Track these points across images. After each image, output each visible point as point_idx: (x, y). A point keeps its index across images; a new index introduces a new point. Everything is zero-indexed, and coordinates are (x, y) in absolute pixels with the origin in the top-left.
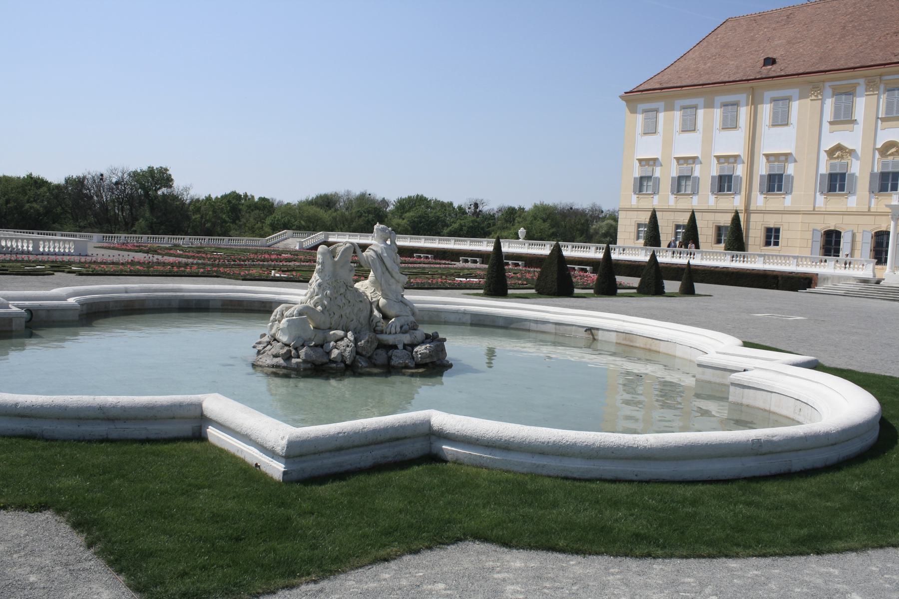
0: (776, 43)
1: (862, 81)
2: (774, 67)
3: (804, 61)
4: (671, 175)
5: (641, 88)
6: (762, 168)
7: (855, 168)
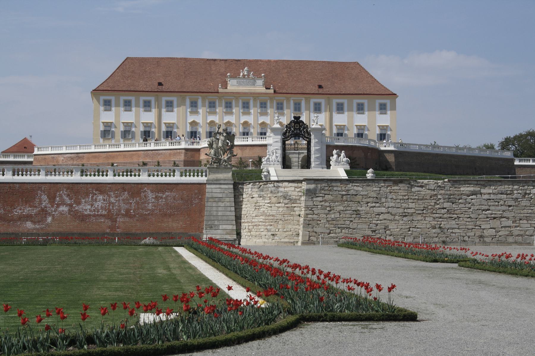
0: (158, 75)
1: (200, 97)
2: (163, 87)
3: (175, 86)
4: (120, 130)
5: (100, 88)
6: (164, 129)
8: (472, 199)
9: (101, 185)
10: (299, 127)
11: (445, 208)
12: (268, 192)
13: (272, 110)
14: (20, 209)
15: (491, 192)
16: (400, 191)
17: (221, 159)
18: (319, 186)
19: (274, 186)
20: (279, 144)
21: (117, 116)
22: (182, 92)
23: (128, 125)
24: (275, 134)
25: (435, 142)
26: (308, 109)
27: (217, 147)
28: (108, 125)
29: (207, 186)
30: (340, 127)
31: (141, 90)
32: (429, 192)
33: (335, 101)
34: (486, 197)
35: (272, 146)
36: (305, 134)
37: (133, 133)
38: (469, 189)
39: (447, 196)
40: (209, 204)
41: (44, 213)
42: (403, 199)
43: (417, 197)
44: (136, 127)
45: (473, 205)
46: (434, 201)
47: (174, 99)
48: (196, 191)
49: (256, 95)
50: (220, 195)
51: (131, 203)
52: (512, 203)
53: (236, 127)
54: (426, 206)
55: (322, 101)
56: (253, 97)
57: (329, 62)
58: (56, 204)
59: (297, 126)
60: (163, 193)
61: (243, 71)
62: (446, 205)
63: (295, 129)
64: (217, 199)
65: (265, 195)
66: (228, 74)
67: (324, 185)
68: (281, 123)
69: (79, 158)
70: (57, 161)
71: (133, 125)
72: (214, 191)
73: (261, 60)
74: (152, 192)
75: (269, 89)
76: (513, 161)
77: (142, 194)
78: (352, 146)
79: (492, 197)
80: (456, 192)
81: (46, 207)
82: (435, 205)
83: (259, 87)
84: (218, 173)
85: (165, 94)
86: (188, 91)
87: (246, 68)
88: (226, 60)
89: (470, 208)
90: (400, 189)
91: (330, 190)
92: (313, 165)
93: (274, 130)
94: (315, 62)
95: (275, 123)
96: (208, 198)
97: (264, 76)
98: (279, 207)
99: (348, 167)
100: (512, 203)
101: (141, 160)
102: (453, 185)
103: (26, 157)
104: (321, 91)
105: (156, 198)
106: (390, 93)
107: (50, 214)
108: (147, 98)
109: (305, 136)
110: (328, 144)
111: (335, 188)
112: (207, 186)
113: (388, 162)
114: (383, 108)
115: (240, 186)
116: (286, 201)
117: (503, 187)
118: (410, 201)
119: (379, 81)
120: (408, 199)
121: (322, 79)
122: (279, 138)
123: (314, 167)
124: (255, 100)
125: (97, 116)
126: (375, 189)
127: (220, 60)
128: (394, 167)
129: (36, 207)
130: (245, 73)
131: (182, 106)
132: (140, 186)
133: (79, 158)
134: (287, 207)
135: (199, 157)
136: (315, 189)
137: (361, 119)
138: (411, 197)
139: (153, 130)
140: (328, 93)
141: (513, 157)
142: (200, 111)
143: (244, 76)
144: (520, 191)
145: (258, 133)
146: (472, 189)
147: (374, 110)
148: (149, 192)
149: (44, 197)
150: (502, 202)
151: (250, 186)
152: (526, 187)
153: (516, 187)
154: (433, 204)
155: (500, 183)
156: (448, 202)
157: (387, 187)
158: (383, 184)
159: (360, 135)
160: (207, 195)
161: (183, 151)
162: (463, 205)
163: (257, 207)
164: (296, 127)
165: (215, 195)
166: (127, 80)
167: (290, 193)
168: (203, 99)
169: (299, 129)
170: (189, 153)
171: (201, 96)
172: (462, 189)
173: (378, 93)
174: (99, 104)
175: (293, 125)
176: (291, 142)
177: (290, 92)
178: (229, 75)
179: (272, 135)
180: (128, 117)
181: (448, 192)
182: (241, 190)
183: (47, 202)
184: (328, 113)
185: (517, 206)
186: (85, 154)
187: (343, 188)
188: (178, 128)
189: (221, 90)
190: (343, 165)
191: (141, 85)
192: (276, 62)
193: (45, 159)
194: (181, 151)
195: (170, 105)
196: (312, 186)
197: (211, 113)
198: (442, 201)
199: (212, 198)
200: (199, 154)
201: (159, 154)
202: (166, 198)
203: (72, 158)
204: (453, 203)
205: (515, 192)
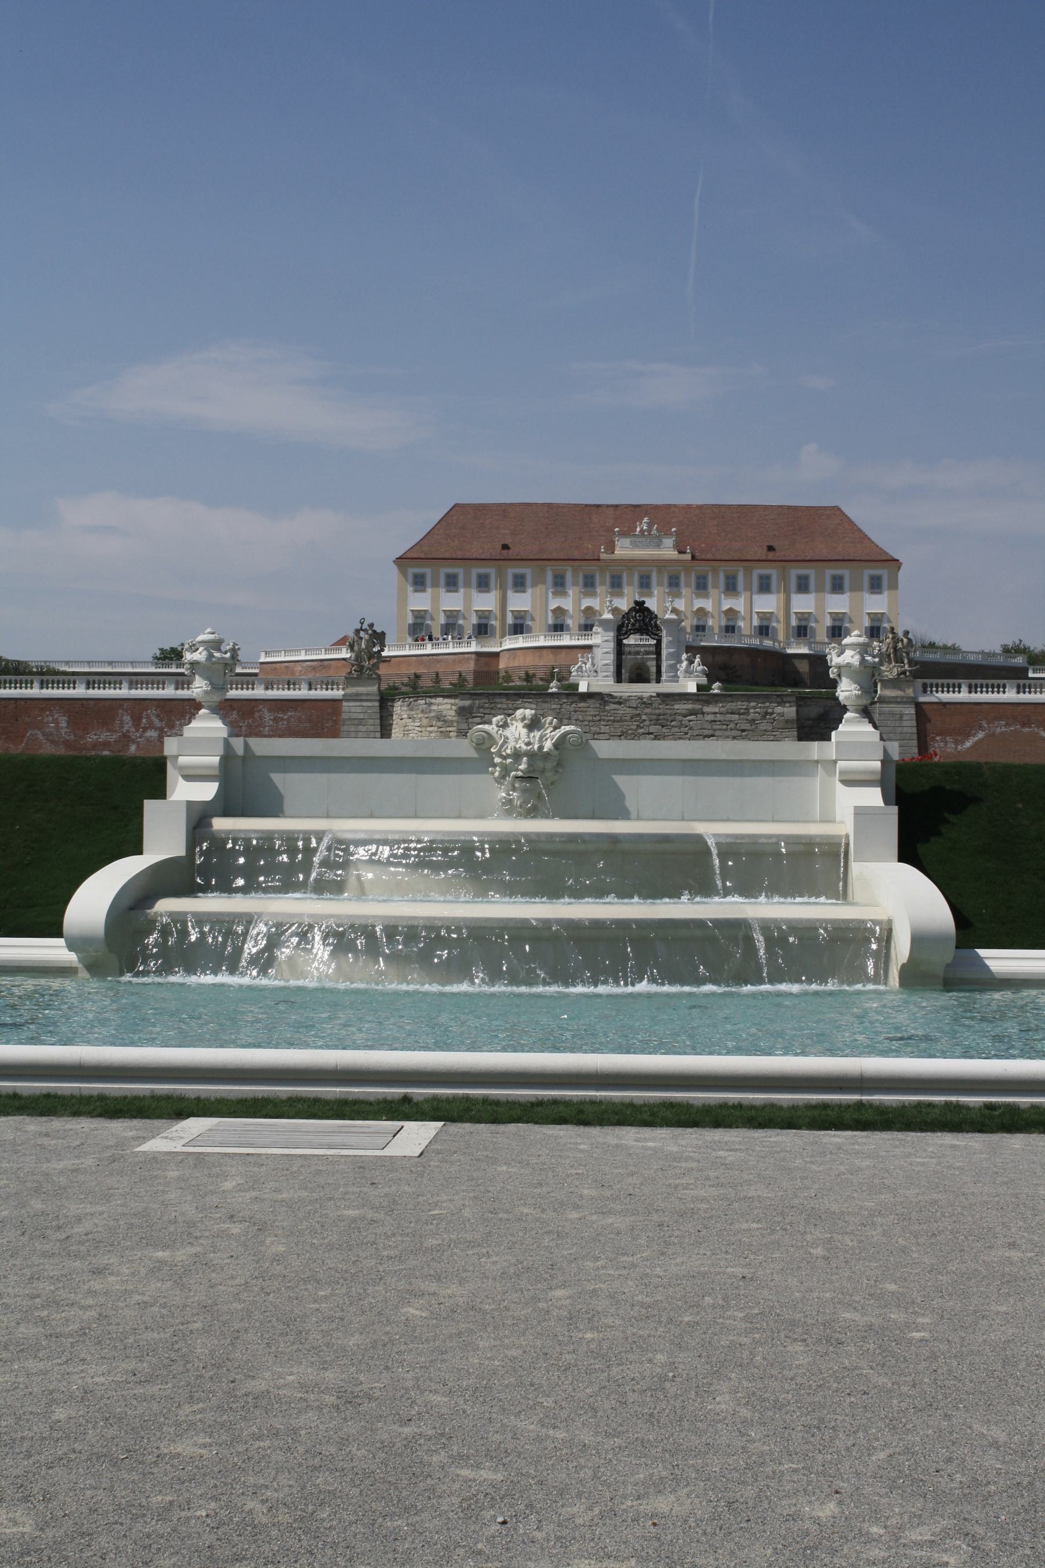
0: (503, 531)
1: (569, 568)
2: (511, 552)
5: (409, 555)
6: (510, 620)
7: (569, 622)
8: (690, 721)
9: (176, 702)
11: (652, 734)
12: (419, 712)
13: (661, 589)
14: (95, 735)
15: (717, 710)
16: (589, 709)
17: (363, 667)
18: (477, 702)
19: (426, 703)
20: (611, 646)
21: (435, 600)
22: (539, 560)
23: (451, 615)
24: (606, 630)
25: (1021, 641)
26: (748, 588)
27: (359, 649)
28: (419, 615)
29: (345, 704)
30: (802, 617)
31: (474, 556)
32: (629, 710)
33: (794, 573)
34: (710, 717)
37: (461, 627)
38: (686, 706)
39: (654, 717)
40: (346, 728)
41: (126, 738)
42: (593, 721)
43: (612, 718)
44: (465, 618)
45: (691, 729)
46: (637, 723)
47: (527, 571)
48: (329, 711)
49: (661, 564)
50: (361, 716)
51: (241, 727)
52: (747, 726)
53: (713, 617)
54: (625, 730)
55: (773, 573)
56: (657, 566)
57: (789, 507)
58: (143, 728)
60: (285, 712)
61: (641, 523)
62: (653, 729)
63: (636, 620)
64: (356, 722)
65: (415, 716)
66: (616, 529)
67: (483, 701)
68: (615, 611)
69: (324, 667)
70: (293, 673)
71: (460, 614)
72: (353, 710)
73: (675, 506)
74: (270, 710)
75: (685, 553)
76: (1026, 670)
77: (257, 715)
78: (729, 647)
79: (719, 717)
80: (667, 711)
81: (128, 731)
82: (637, 729)
83: (667, 550)
84: (359, 686)
85: (512, 563)
86: (551, 558)
87: (646, 520)
88: (617, 506)
89: (686, 734)
90: (589, 707)
91: (492, 708)
92: (664, 677)
93: (604, 624)
94: (766, 508)
95: (606, 611)
96: (344, 720)
97: (675, 531)
98: (430, 732)
99: (704, 680)
100: (747, 726)
101: (413, 671)
102: (663, 701)
103: (174, 666)
104: (771, 555)
105: (275, 720)
106: (889, 558)
107: (134, 741)
108: (483, 571)
110: (689, 644)
111: (499, 706)
112: (345, 704)
113: (798, 672)
114: (876, 586)
115: (389, 704)
116: (440, 724)
117: (734, 704)
118: (602, 723)
119: (871, 538)
120: (600, 720)
121: (775, 535)
122: (611, 635)
123: (666, 681)
124: (660, 571)
125: (403, 600)
126: (554, 706)
127: (608, 506)
128: (808, 682)
129: (116, 731)
130: (645, 528)
131: (540, 586)
132: (253, 703)
133: (324, 667)
134: (441, 732)
135: (498, 665)
136: (471, 707)
137: (768, 603)
138: (605, 718)
139: (493, 622)
140: (784, 558)
141: (1026, 665)
142: (570, 592)
143: (642, 531)
144: (758, 710)
145: (580, 626)
146: (690, 706)
147: (861, 589)
148: (265, 710)
149: (127, 718)
150: (732, 726)
151: (399, 703)
152: (767, 704)
153: (753, 704)
154: (634, 727)
155: (730, 699)
156: (656, 725)
157: (572, 703)
158: (565, 701)
159: (730, 629)
160: (344, 716)
161: (473, 656)
162: (676, 729)
163: (406, 732)
165: (354, 716)
166: (453, 541)
167: (445, 713)
168: (575, 571)
170: (483, 660)
171: (571, 566)
172: (676, 707)
173: (868, 558)
174: (407, 581)
176: (631, 640)
177: (718, 558)
178: (618, 531)
179: (600, 630)
180: (452, 601)
181: (657, 711)
182: (391, 709)
183: (130, 724)
184: (782, 596)
185: (752, 730)
186: (332, 662)
187: (510, 706)
188: (533, 619)
189: (603, 556)
190: (697, 676)
191: (475, 549)
192: (700, 507)
193: (275, 669)
194: (470, 655)
195: (520, 584)
196: (467, 703)
197: (587, 595)
198: (647, 723)
199: (350, 719)
200: (498, 661)
201: (439, 661)
202: (288, 720)
203: (314, 668)
204: (663, 727)
205: (752, 711)
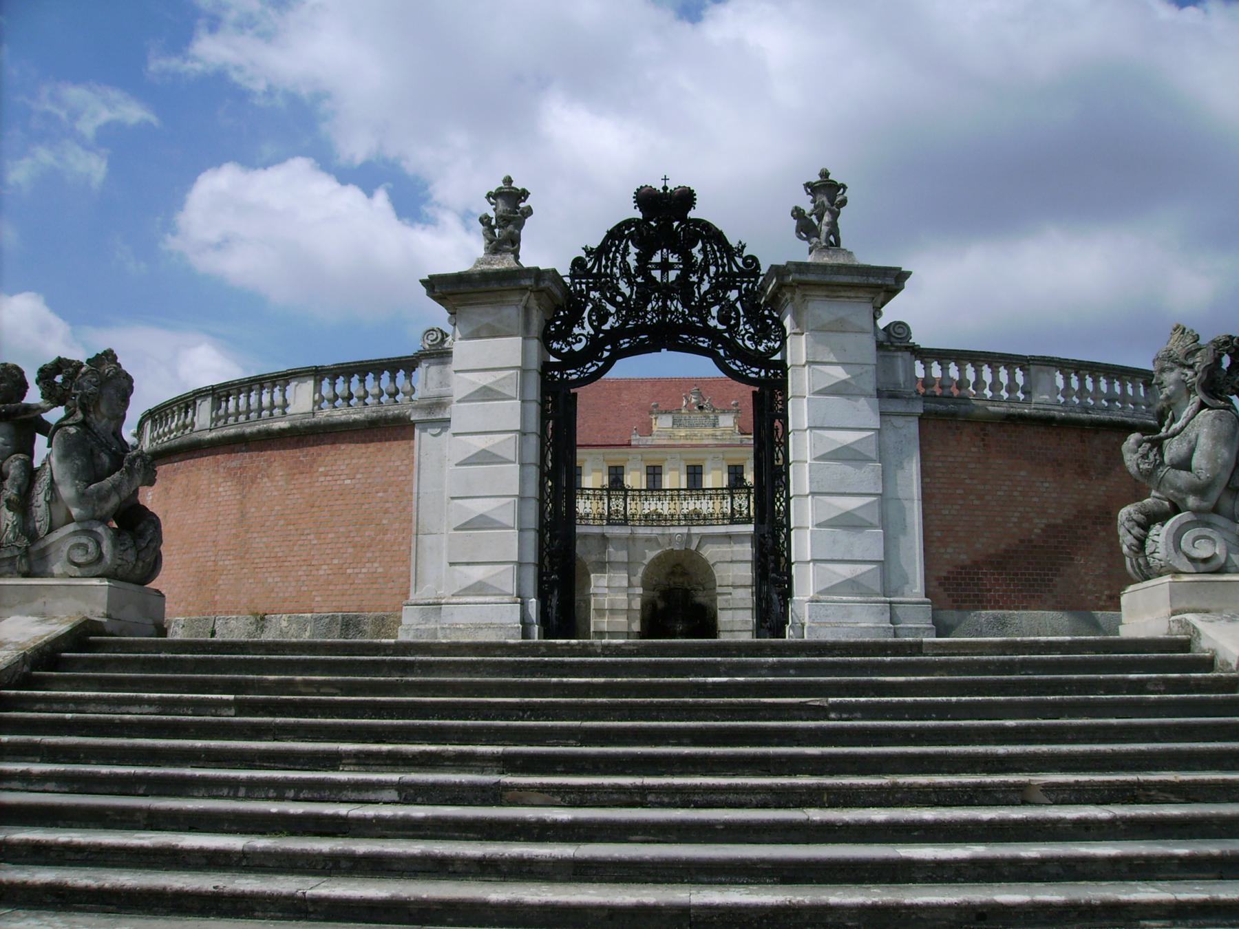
10: (682, 278)
35: (446, 435)
36: (732, 329)
59: (665, 266)
109: (730, 345)
164: (657, 274)
169: (683, 288)
175: (632, 260)
189: (635, 439)
